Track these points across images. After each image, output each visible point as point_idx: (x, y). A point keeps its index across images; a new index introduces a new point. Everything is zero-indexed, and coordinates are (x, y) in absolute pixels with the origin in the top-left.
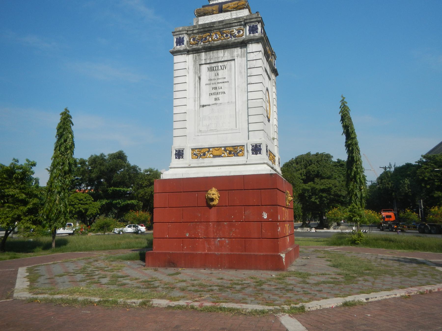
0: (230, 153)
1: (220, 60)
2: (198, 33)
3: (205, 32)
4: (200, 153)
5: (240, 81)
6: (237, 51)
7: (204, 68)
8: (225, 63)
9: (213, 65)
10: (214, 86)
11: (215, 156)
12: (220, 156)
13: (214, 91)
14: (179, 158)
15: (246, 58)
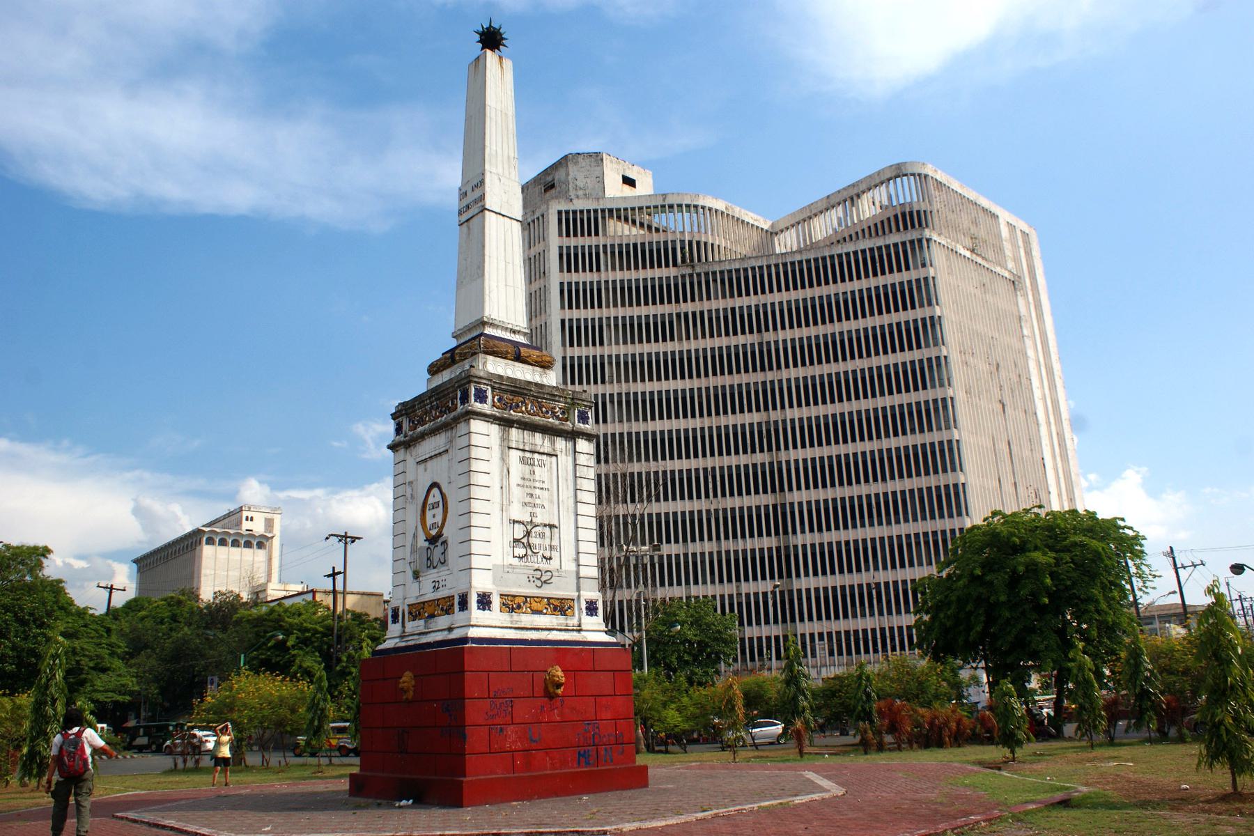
0: (555, 609)
1: (538, 449)
2: (506, 391)
3: (519, 394)
4: (512, 604)
5: (566, 494)
6: (561, 443)
7: (515, 455)
8: (545, 457)
9: (528, 455)
10: (529, 491)
11: (535, 612)
12: (540, 612)
13: (528, 500)
14: (484, 609)
15: (570, 459)
